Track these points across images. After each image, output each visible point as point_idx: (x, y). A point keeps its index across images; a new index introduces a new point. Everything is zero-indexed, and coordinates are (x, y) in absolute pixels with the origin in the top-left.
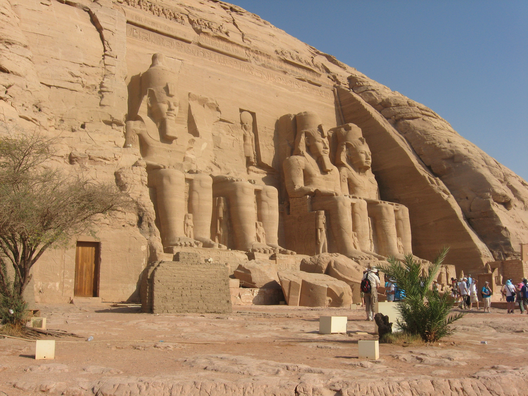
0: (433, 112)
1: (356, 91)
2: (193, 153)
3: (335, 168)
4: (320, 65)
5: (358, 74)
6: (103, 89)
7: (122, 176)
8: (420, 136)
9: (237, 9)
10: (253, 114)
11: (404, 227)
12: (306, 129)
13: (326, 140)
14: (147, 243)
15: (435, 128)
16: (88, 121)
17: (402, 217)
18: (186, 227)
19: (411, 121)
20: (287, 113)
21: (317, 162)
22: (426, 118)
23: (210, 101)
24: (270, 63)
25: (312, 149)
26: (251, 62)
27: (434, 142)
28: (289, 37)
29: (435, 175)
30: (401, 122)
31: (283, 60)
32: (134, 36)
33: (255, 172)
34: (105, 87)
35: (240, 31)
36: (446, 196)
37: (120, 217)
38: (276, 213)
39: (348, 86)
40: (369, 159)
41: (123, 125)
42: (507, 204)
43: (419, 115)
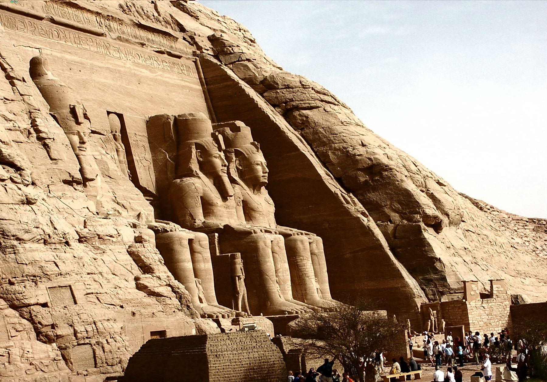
4: (170, 19)
7: (142, 257)
8: (325, 137)
10: (120, 117)
12: (196, 139)
13: (222, 154)
15: (342, 123)
17: (316, 251)
22: (328, 107)
24: (123, 33)
29: (348, 191)
38: (209, 266)
40: (266, 173)
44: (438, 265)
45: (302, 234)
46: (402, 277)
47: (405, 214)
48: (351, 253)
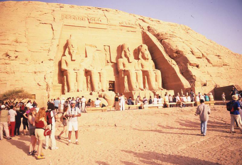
6: (50, 50)
10: (109, 46)
15: (173, 41)
19: (165, 40)
22: (171, 38)
23: (93, 45)
25: (126, 56)
26: (108, 29)
30: (162, 41)
31: (120, 26)
36: (173, 66)
42: (197, 66)
43: (168, 37)
44: (194, 77)
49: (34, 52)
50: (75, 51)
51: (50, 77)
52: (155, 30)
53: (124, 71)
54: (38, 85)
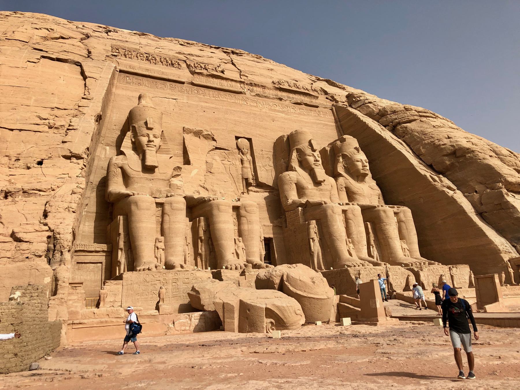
0: (431, 112)
1: (353, 106)
2: (181, 179)
3: (332, 180)
4: (318, 89)
5: (356, 91)
8: (418, 137)
9: (237, 51)
10: (250, 140)
11: (407, 229)
14: (52, 274)
15: (434, 127)
16: (47, 158)
17: (404, 219)
18: (156, 250)
19: (408, 124)
20: (281, 134)
21: (310, 175)
22: (424, 119)
23: (205, 133)
26: (245, 94)
27: (432, 140)
28: (289, 69)
30: (399, 127)
32: (127, 83)
33: (254, 192)
34: (72, 126)
35: (239, 69)
37: (25, 249)
39: (346, 103)
41: (83, 158)
43: (416, 117)
45: (394, 207)
46: (483, 234)
47: (489, 184)
48: (441, 220)
49: (12, 130)
50: (157, 142)
51: (68, 209)
52: (370, 103)
53: (307, 206)
54: (11, 239)
